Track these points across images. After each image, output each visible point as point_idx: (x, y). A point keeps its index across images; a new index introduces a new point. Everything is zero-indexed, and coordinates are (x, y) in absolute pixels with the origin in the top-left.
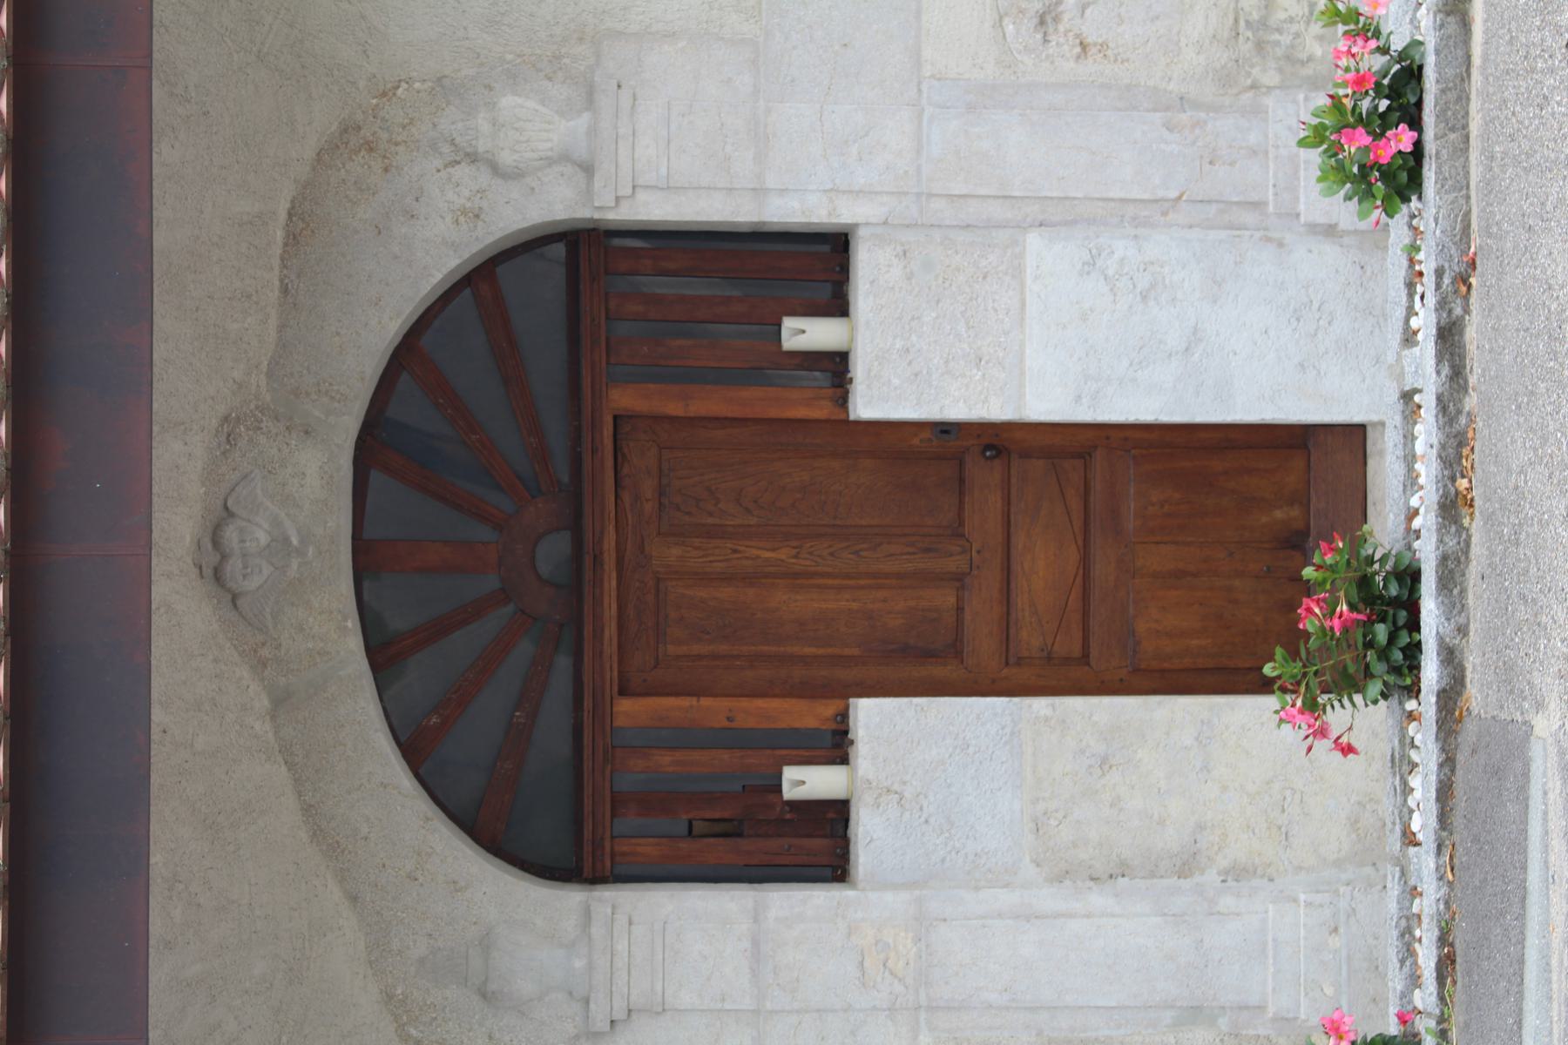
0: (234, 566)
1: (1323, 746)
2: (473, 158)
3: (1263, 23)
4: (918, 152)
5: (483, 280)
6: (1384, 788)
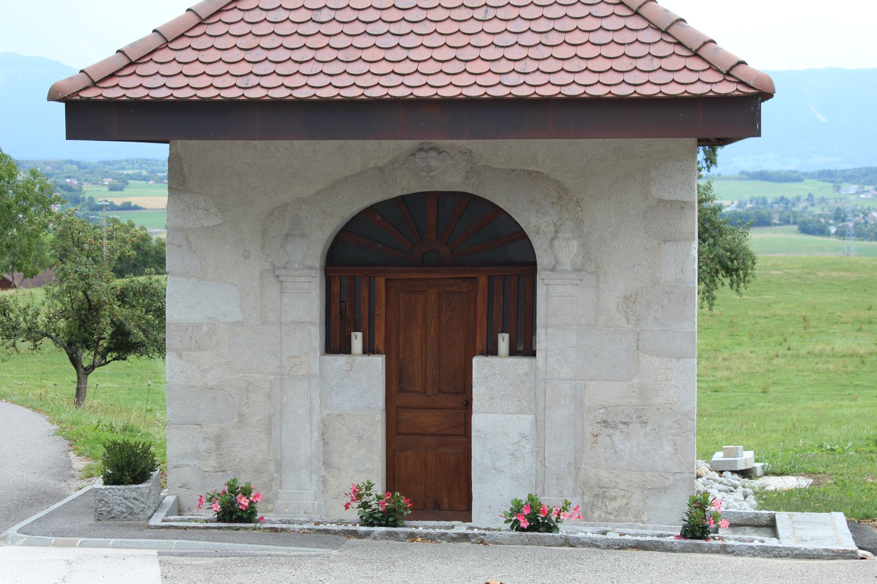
0: (423, 154)
1: (348, 500)
2: (557, 232)
3: (605, 497)
4: (560, 379)
5: (520, 236)
6: (335, 518)
